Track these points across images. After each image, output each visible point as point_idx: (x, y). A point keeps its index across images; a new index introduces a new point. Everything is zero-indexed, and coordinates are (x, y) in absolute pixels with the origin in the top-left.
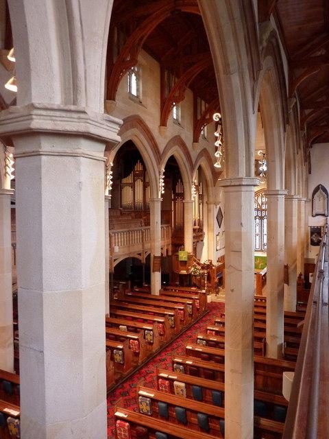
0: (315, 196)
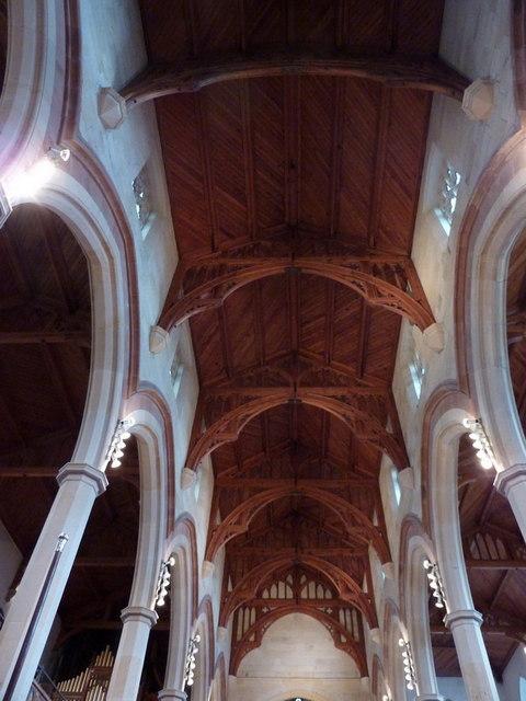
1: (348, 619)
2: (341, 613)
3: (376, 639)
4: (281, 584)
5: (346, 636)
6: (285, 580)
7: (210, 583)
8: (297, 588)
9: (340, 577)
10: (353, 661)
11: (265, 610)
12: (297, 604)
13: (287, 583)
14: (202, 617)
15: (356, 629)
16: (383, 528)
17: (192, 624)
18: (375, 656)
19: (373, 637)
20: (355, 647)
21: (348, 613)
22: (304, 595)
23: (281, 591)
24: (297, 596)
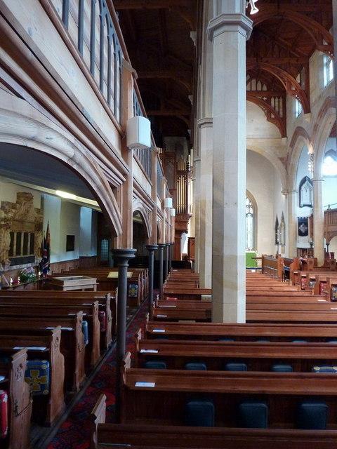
0: (303, 187)
1: (277, 103)
2: (272, 100)
3: (308, 120)
5: (275, 115)
9: (284, 77)
15: (281, 110)
20: (280, 119)
21: (277, 100)
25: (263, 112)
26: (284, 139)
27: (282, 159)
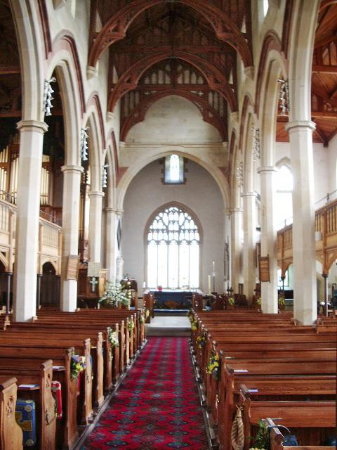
1: (216, 100)
2: (210, 95)
4: (161, 72)
5: (213, 113)
6: (164, 69)
7: (95, 84)
8: (173, 76)
10: (217, 132)
11: (147, 93)
12: (174, 89)
13: (165, 72)
14: (91, 109)
15: (222, 107)
16: (249, 35)
17: (82, 117)
18: (234, 129)
19: (232, 117)
20: (219, 122)
22: (180, 81)
23: (161, 79)
24: (174, 82)
25: (198, 110)
26: (225, 144)
27: (222, 169)
